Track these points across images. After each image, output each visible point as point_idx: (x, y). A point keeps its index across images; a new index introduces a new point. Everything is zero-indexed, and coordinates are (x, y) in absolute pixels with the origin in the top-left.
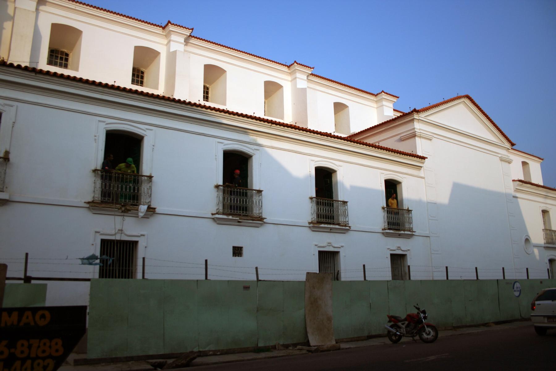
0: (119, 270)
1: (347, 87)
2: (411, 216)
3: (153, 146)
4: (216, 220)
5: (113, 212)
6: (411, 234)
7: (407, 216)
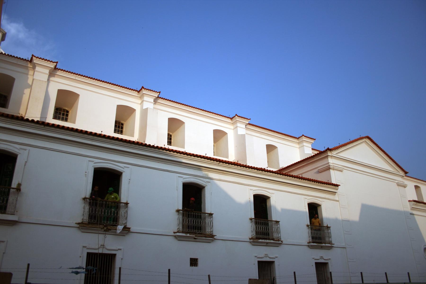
0: (100, 277)
1: (276, 133)
2: (330, 232)
3: (129, 180)
4: (177, 237)
5: (97, 231)
6: (331, 246)
7: (327, 231)
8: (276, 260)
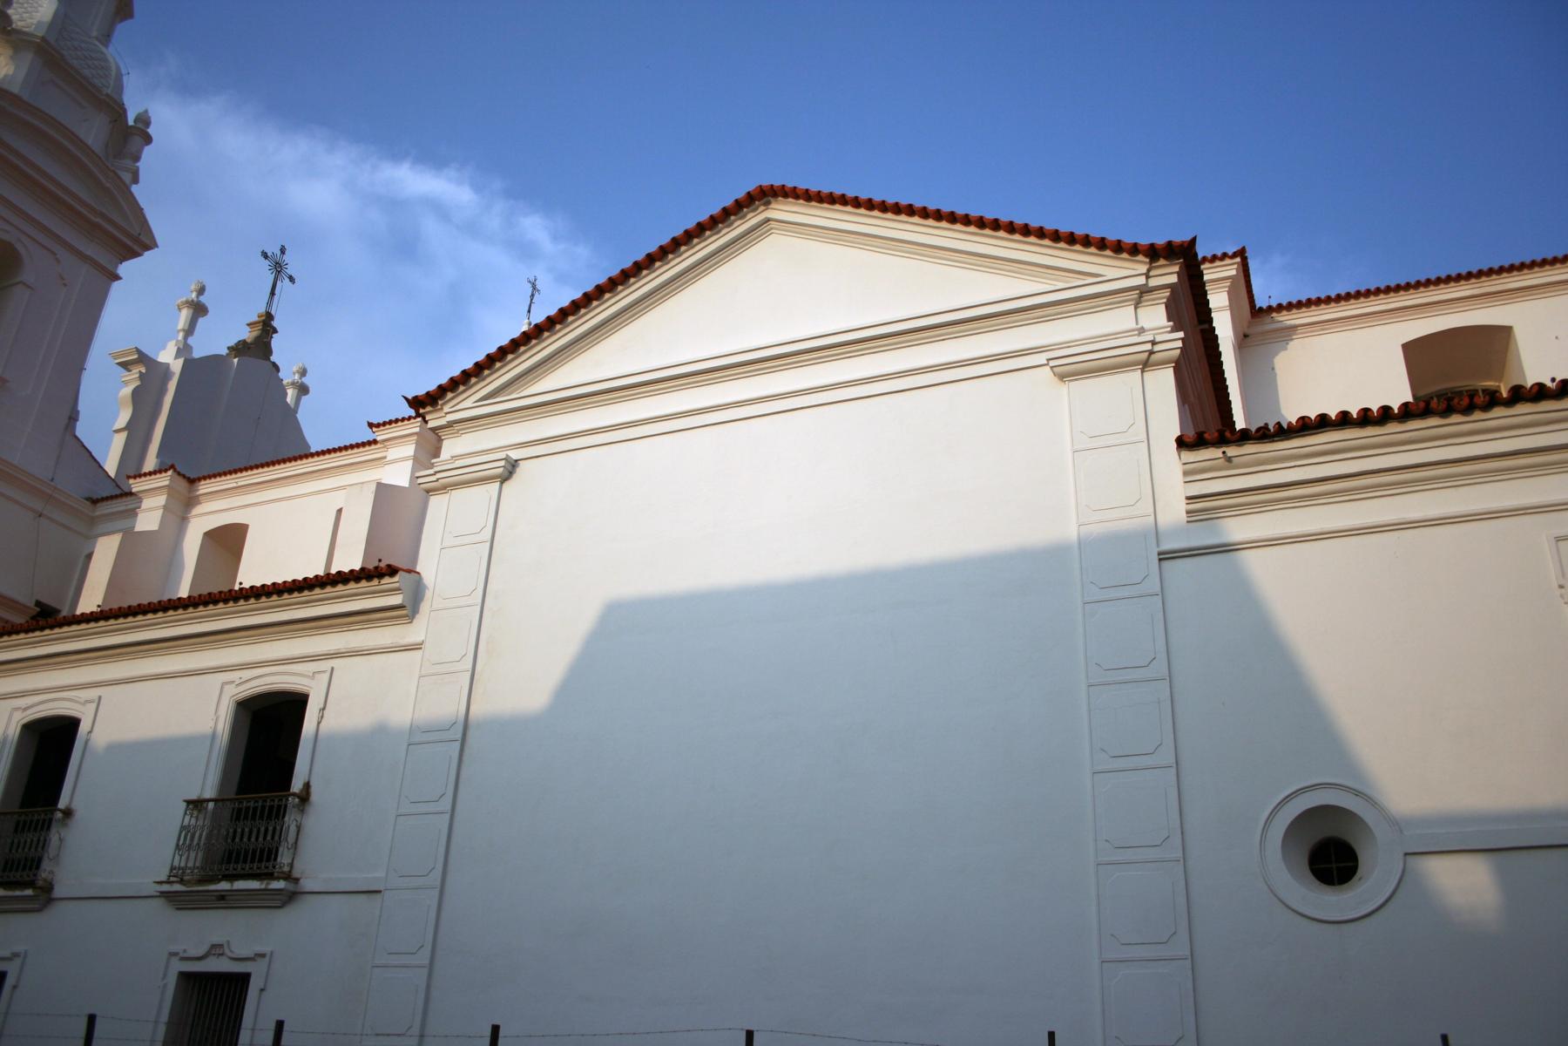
8: (256, 970)
